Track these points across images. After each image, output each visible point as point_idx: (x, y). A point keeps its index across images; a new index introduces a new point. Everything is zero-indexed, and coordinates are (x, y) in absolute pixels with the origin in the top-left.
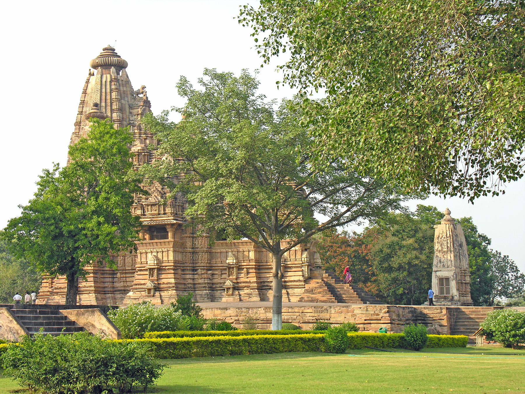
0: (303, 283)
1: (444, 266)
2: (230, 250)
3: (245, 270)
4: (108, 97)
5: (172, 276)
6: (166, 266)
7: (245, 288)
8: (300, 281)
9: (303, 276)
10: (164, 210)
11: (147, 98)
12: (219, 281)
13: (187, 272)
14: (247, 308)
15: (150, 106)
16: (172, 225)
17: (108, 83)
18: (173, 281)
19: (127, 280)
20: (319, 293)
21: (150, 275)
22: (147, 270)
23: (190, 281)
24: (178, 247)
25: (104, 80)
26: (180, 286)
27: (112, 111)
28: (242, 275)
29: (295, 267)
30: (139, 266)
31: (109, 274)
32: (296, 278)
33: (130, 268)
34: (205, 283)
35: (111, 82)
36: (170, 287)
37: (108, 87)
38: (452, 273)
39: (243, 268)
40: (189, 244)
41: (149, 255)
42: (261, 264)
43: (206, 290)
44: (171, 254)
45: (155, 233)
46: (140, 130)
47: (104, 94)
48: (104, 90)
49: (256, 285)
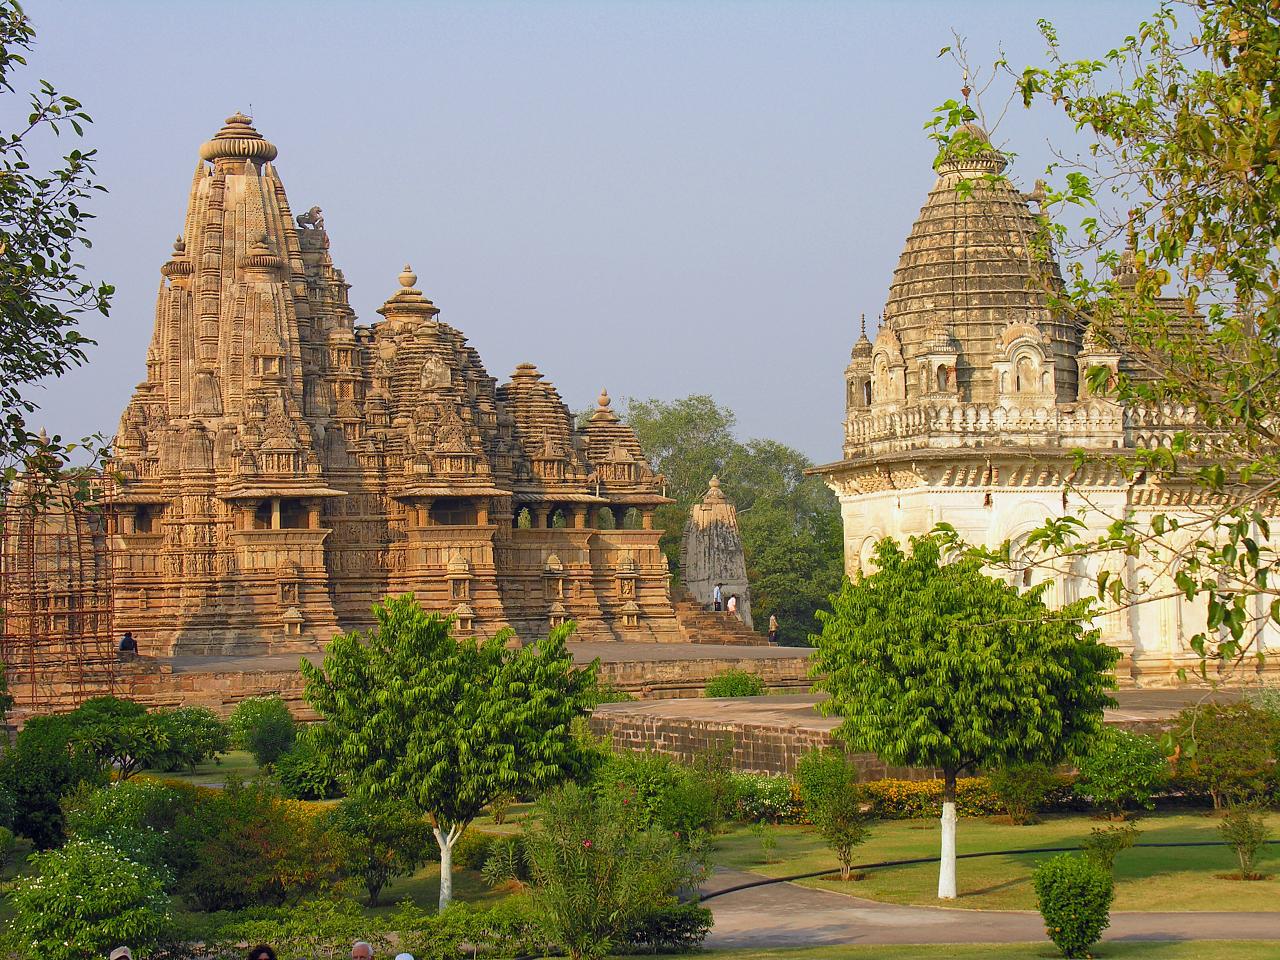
1: (732, 576)
14: (773, 659)
18: (498, 604)
25: (265, 190)
29: (652, 580)
32: (658, 601)
36: (496, 616)
38: (743, 589)
41: (444, 554)
47: (271, 219)
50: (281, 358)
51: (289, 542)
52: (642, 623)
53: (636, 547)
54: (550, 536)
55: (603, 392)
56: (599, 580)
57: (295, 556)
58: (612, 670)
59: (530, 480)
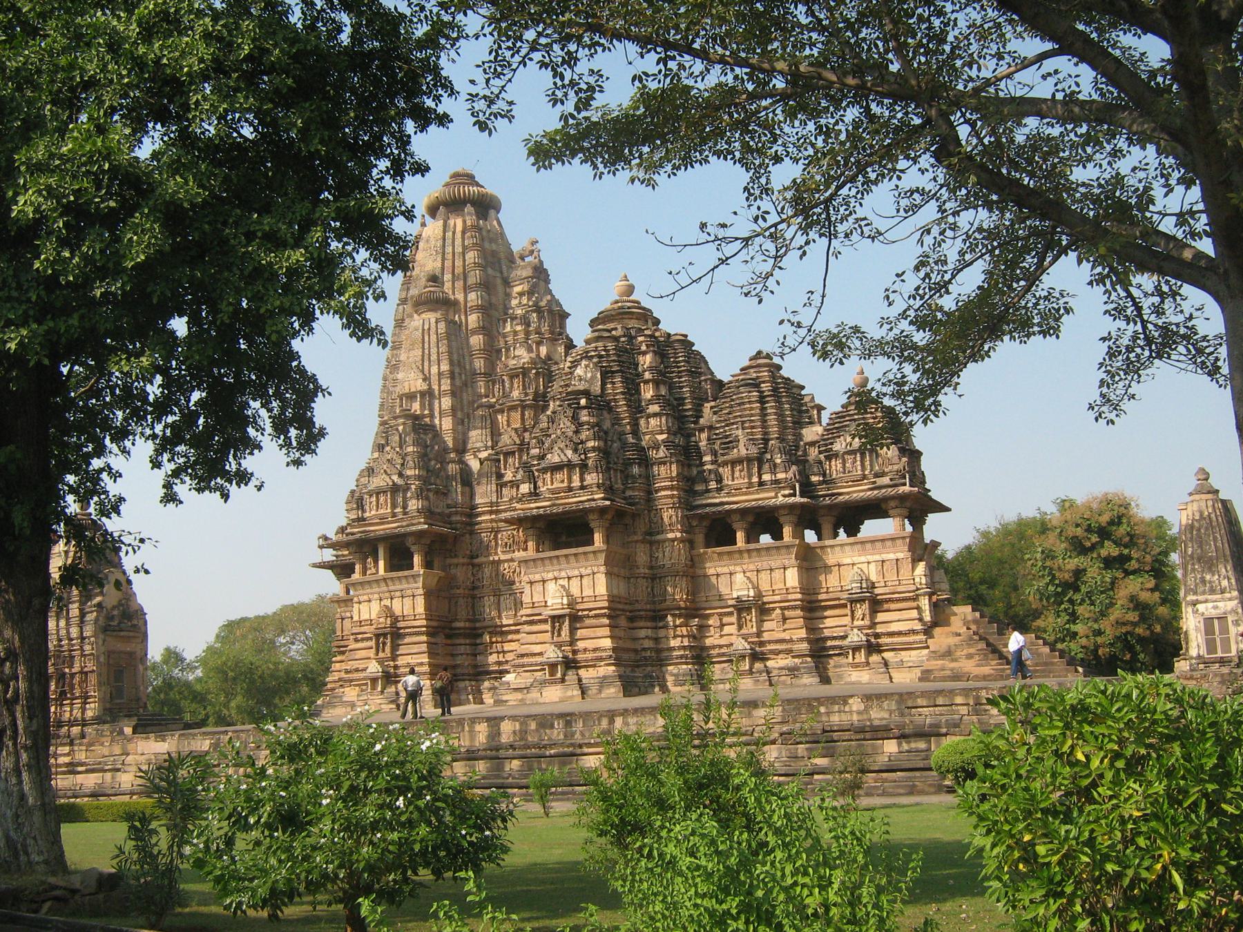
0: (922, 637)
2: (738, 568)
3: (778, 611)
4: (459, 263)
5: (606, 631)
6: (590, 610)
7: (781, 656)
8: (913, 632)
9: (921, 620)
10: (582, 480)
11: (541, 262)
12: (716, 642)
13: (642, 624)
15: (547, 281)
16: (602, 511)
17: (458, 235)
18: (607, 643)
19: (506, 649)
20: (969, 657)
21: (553, 633)
22: (545, 621)
24: (618, 567)
26: (625, 656)
27: (466, 289)
30: (529, 611)
31: (466, 636)
33: (511, 622)
34: (684, 648)
35: (463, 233)
36: (601, 659)
37: (458, 242)
39: (774, 609)
40: (642, 557)
41: (551, 586)
43: (687, 663)
44: (601, 580)
45: (564, 538)
46: (528, 325)
48: (449, 249)
49: (805, 645)
50: (423, 394)
51: (392, 588)
52: (875, 658)
53: (877, 557)
54: (746, 555)
55: (858, 370)
56: (812, 607)
57: (397, 606)
58: (568, 724)
59: (719, 490)
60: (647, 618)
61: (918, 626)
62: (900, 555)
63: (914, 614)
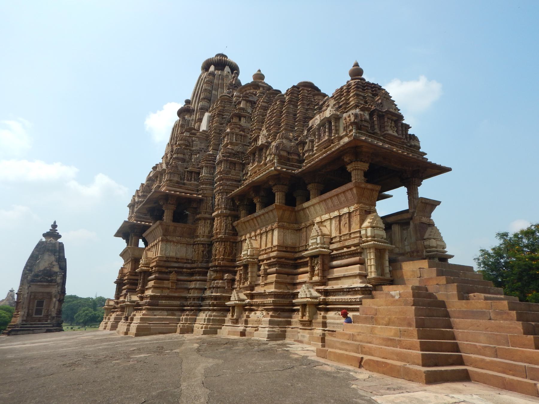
9: (363, 276)
23: (196, 294)
28: (260, 281)
42: (297, 255)
53: (336, 213)
60: (199, 273)
61: (357, 284)
62: (352, 209)
63: (355, 269)
